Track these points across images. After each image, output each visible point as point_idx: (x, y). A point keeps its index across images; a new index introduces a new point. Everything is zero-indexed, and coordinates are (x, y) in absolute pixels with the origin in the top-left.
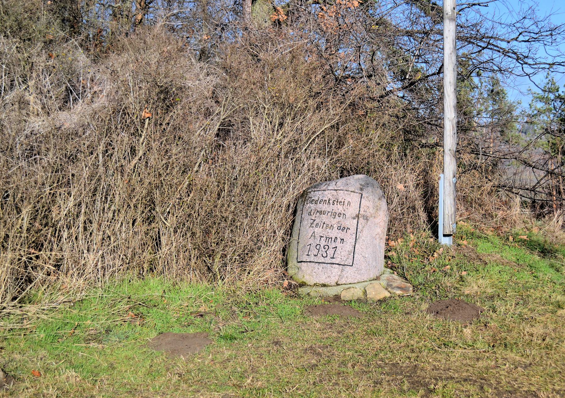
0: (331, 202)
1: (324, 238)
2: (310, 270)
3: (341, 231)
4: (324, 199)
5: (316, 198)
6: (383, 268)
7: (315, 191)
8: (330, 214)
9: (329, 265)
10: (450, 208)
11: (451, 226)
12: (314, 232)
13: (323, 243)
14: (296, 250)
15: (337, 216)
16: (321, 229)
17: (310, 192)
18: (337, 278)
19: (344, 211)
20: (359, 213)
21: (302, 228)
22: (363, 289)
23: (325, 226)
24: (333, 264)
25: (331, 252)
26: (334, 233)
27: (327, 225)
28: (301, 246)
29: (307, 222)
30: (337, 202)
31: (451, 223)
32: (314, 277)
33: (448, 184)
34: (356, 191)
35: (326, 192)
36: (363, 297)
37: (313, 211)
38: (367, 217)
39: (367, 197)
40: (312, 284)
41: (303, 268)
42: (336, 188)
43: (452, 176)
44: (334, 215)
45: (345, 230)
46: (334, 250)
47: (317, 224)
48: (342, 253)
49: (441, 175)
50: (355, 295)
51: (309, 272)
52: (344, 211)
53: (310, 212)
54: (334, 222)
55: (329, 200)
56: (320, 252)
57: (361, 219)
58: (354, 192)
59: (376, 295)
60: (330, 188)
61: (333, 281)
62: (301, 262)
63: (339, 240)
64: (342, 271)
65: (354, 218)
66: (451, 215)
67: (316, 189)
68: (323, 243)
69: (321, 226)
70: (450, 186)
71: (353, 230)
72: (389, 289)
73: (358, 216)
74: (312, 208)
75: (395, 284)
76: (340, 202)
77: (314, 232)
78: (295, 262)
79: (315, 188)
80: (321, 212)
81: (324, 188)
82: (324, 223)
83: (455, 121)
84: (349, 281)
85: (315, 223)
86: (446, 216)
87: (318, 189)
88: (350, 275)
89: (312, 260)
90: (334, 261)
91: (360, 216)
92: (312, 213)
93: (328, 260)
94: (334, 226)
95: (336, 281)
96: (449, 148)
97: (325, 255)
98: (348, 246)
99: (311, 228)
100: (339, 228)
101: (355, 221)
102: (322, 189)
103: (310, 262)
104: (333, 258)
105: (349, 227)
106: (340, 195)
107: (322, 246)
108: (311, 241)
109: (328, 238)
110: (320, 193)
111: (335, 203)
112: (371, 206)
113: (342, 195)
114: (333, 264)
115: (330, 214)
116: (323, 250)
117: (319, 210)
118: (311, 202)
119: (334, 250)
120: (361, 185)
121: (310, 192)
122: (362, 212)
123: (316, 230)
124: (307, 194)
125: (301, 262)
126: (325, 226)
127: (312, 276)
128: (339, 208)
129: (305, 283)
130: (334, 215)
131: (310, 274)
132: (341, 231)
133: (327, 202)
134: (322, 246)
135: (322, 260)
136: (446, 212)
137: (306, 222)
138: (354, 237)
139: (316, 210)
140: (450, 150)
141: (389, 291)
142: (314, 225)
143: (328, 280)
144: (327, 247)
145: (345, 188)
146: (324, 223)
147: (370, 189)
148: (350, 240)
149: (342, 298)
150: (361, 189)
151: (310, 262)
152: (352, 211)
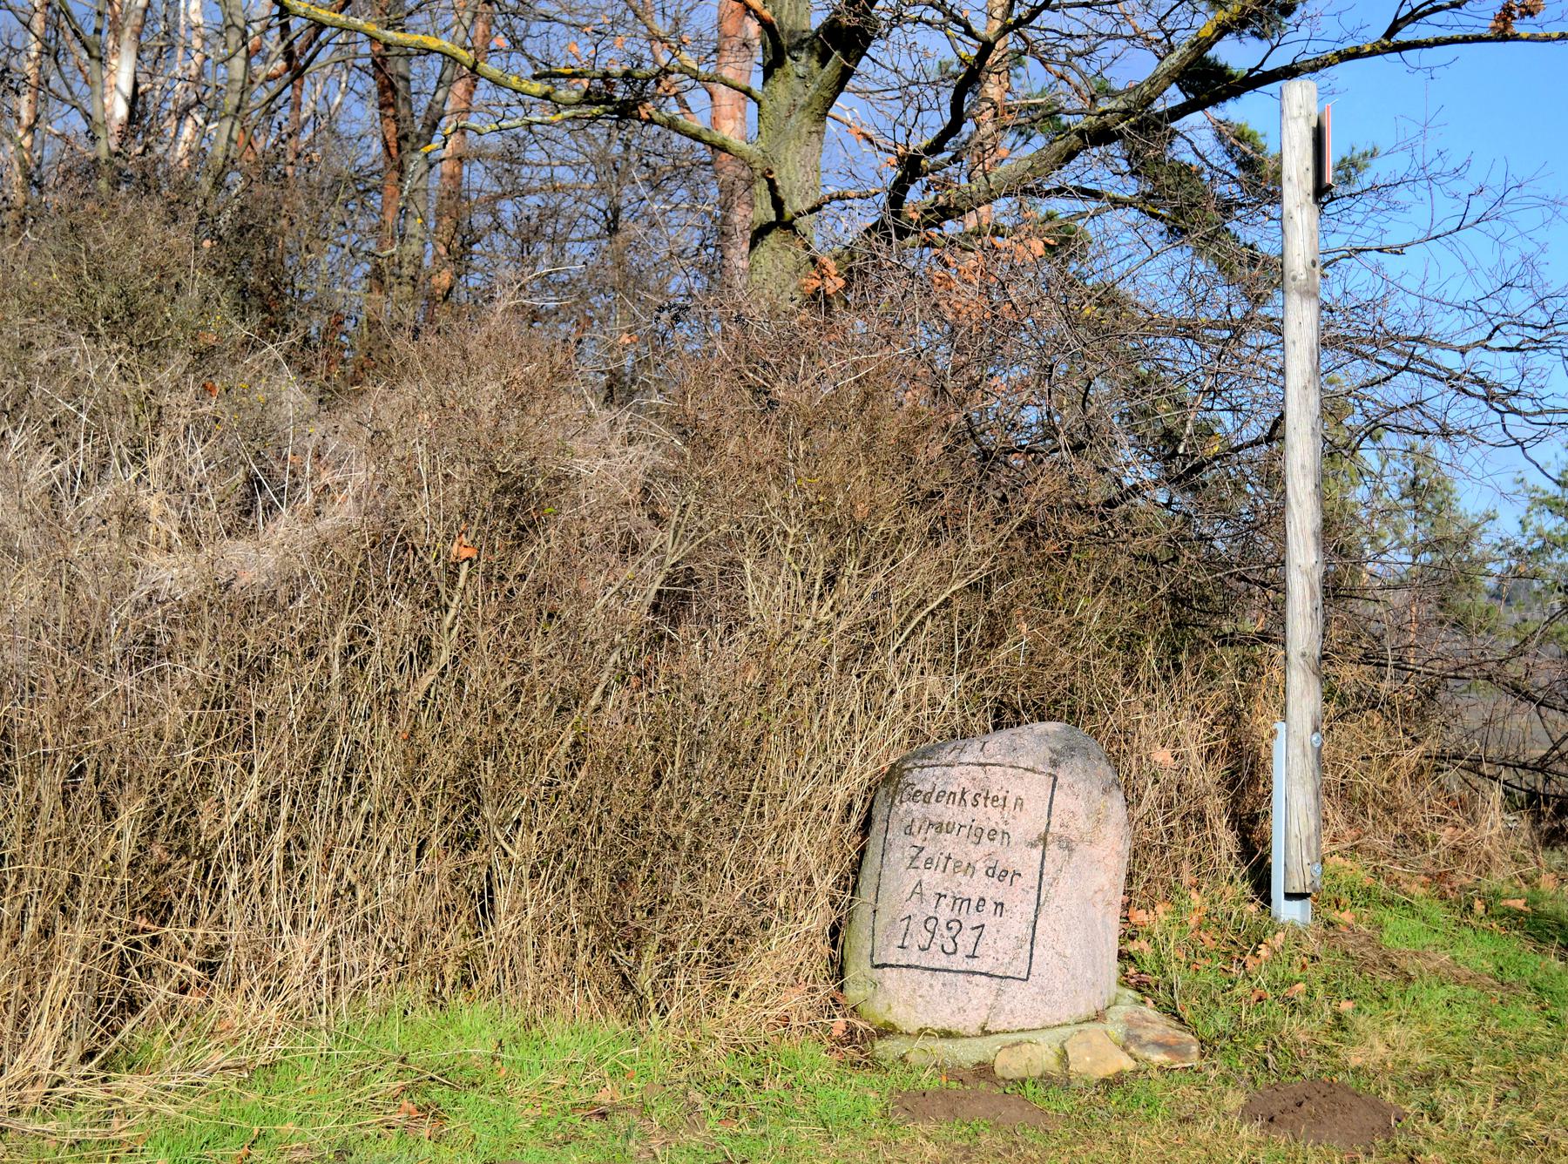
0: (969, 797)
1: (949, 900)
2: (908, 989)
3: (995, 879)
4: (949, 789)
5: (927, 787)
6: (1115, 988)
7: (923, 767)
8: (964, 831)
10: (1303, 819)
11: (1307, 869)
12: (920, 883)
13: (945, 913)
14: (868, 932)
15: (985, 839)
16: (939, 875)
17: (910, 770)
18: (984, 1013)
19: (1006, 823)
20: (1047, 831)
21: (886, 872)
22: (1056, 1046)
23: (951, 864)
24: (974, 973)
25: (966, 939)
26: (977, 886)
27: (958, 864)
28: (882, 920)
29: (899, 854)
30: (986, 798)
31: (1306, 861)
32: (920, 1009)
33: (1298, 751)
34: (1040, 768)
35: (955, 771)
36: (1057, 1069)
37: (917, 824)
38: (1070, 841)
39: (1071, 786)
40: (914, 1029)
41: (888, 984)
42: (982, 760)
43: (1309, 727)
44: (978, 834)
45: (1008, 879)
47: (929, 861)
49: (1280, 727)
50: (1035, 1062)
51: (904, 994)
52: (1006, 823)
53: (910, 827)
54: (977, 854)
55: (963, 793)
56: (938, 940)
57: (1053, 849)
58: (1033, 771)
59: (1094, 1063)
61: (972, 1023)
62: (884, 966)
63: (990, 906)
64: (998, 995)
65: (1033, 845)
66: (1308, 838)
67: (926, 762)
68: (945, 913)
70: (1305, 755)
71: (1030, 878)
72: (1133, 1049)
73: (1045, 840)
74: (916, 814)
75: (1148, 1035)
77: (920, 883)
78: (866, 966)
79: (924, 757)
80: (939, 827)
81: (950, 758)
82: (949, 858)
83: (1317, 575)
84: (1019, 1023)
86: (1293, 841)
87: (933, 762)
88: (1020, 1007)
89: (913, 962)
90: (974, 965)
91: (1049, 839)
92: (915, 829)
93: (959, 962)
94: (978, 866)
95: (980, 1022)
96: (1300, 649)
97: (950, 948)
98: (1016, 923)
100: (991, 872)
101: (1036, 854)
102: (944, 761)
103: (908, 966)
105: (1018, 868)
106: (993, 779)
107: (942, 922)
108: (911, 908)
109: (960, 901)
110: (938, 771)
111: (981, 800)
112: (1081, 812)
113: (998, 780)
114: (974, 973)
116: (946, 933)
117: (934, 819)
118: (913, 798)
120: (1053, 751)
121: (910, 770)
122: (1055, 828)
123: (926, 876)
124: (901, 776)
125: (884, 966)
126: (951, 864)
127: (915, 1007)
128: (990, 816)
129: (893, 1025)
130: (978, 834)
131: (904, 999)
132: (995, 879)
134: (942, 922)
135: (942, 961)
136: (1294, 830)
139: (925, 819)
140: (1303, 655)
141: (1131, 1055)
142: (920, 863)
143: (959, 1018)
145: (1008, 760)
146: (949, 858)
147: (1078, 762)
148: (1021, 908)
149: (999, 1073)
150: (1054, 764)
151: (908, 966)
152: (1028, 823)
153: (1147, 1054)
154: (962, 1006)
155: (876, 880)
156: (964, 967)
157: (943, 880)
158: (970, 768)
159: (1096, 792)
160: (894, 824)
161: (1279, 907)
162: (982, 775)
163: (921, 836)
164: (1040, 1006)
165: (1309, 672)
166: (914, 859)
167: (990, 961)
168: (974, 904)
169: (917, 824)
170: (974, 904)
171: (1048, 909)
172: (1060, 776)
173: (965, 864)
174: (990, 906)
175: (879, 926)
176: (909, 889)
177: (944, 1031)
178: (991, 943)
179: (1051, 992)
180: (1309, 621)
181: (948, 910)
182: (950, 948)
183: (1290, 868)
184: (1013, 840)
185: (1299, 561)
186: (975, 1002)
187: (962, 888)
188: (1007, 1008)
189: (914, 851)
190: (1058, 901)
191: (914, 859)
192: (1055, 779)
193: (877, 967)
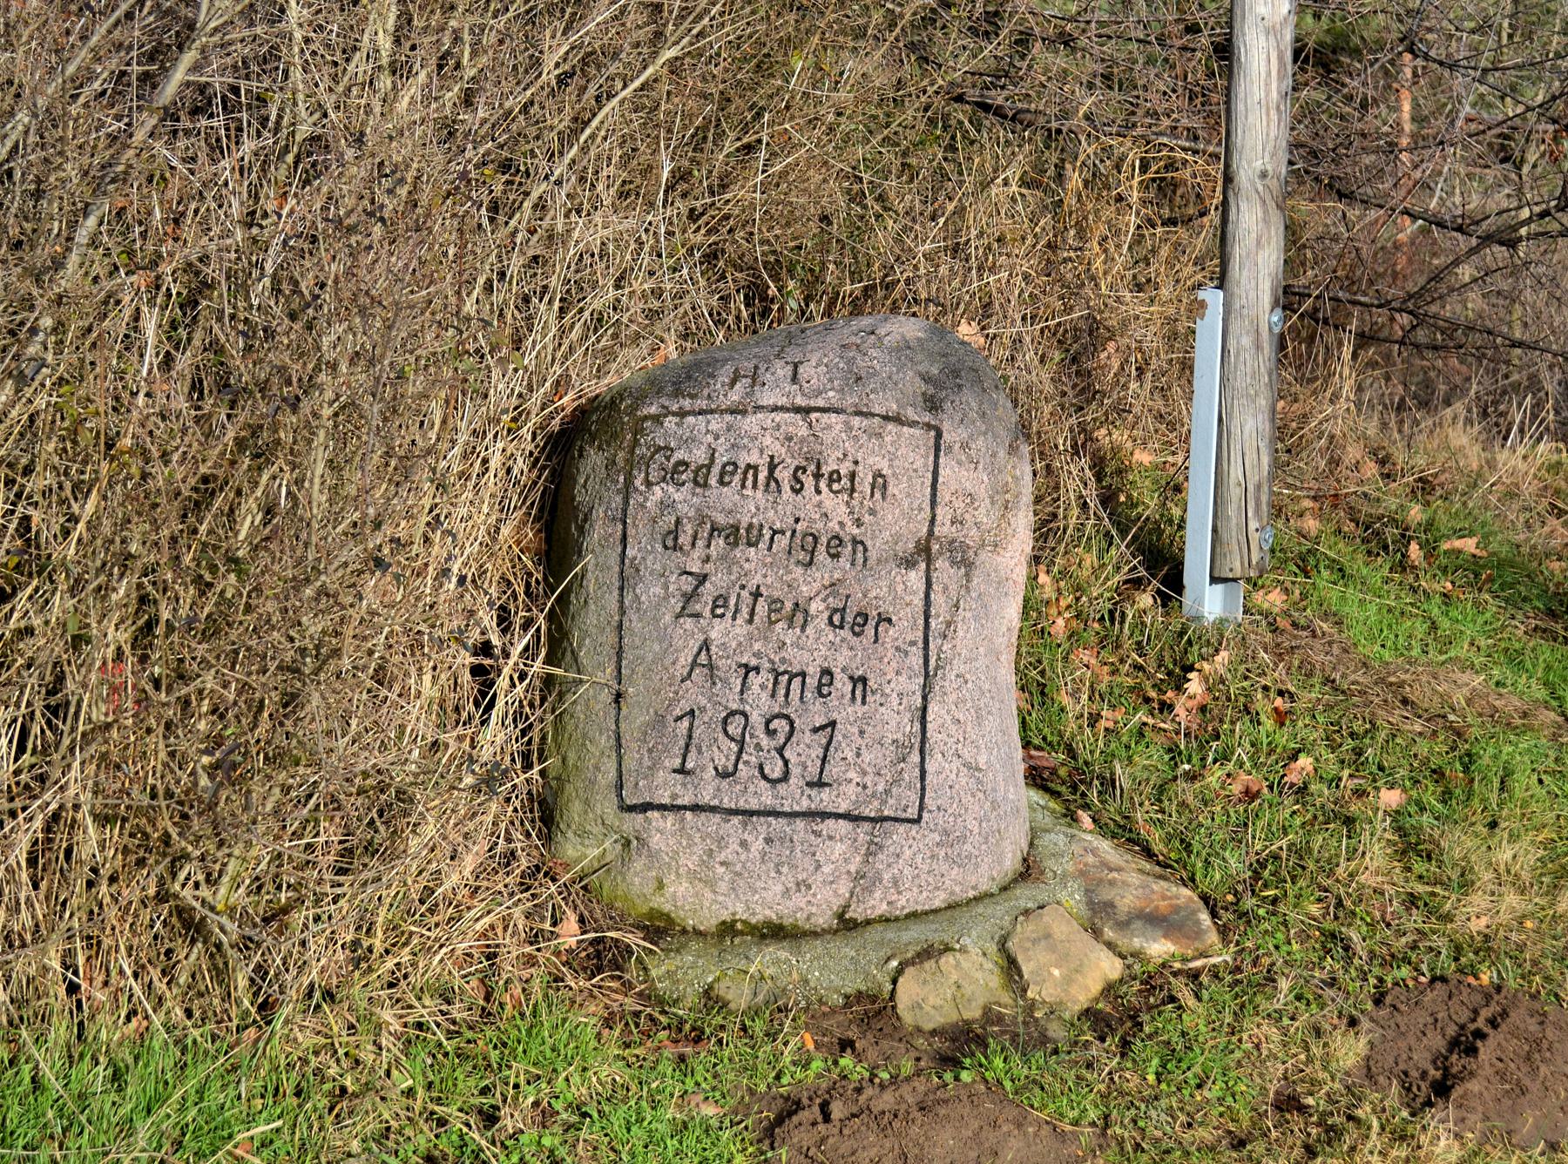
0: (784, 475)
1: (765, 677)
2: (699, 850)
3: (845, 633)
4: (744, 459)
5: (699, 455)
7: (682, 414)
8: (782, 542)
9: (800, 824)
10: (1251, 457)
11: (1254, 537)
12: (706, 645)
13: (760, 703)
14: (605, 741)
15: (821, 555)
16: (741, 629)
17: (657, 419)
18: (844, 888)
19: (858, 523)
20: (931, 533)
21: (634, 622)
22: (992, 948)
23: (762, 607)
24: (825, 815)
25: (804, 752)
26: (815, 647)
27: (775, 605)
28: (636, 718)
29: (656, 589)
30: (817, 476)
31: (1253, 525)
32: (723, 887)
33: (1246, 341)
34: (911, 413)
35: (751, 423)
36: (1006, 998)
37: (689, 529)
38: (965, 548)
39: (965, 446)
40: (709, 922)
41: (656, 841)
42: (800, 401)
43: (1267, 300)
44: (808, 547)
45: (869, 630)
46: (822, 738)
47: (720, 601)
48: (867, 757)
49: (1213, 298)
50: (968, 990)
51: (690, 862)
52: (858, 523)
53: (675, 532)
54: (810, 584)
55: (772, 467)
57: (941, 563)
58: (897, 420)
59: (1068, 980)
60: (768, 398)
61: (819, 907)
62: (646, 807)
63: (842, 685)
64: (869, 854)
65: (909, 564)
66: (1258, 487)
67: (687, 403)
68: (760, 703)
69: (745, 611)
70: (1258, 347)
71: (905, 628)
72: (1109, 933)
73: (928, 550)
74: (683, 509)
75: (1127, 901)
76: (834, 477)
77: (706, 645)
78: (607, 807)
79: (677, 393)
80: (733, 535)
81: (735, 396)
84: (907, 901)
86: (1235, 493)
87: (702, 403)
88: (914, 875)
89: (706, 798)
90: (824, 799)
91: (935, 547)
92: (685, 539)
93: (795, 796)
94: (814, 607)
95: (836, 904)
96: (1258, 164)
97: (775, 770)
99: (688, 623)
101: (915, 578)
102: (725, 403)
103: (696, 808)
104: (820, 784)
106: (827, 438)
107: (756, 718)
108: (694, 694)
110: (716, 423)
111: (809, 481)
112: (982, 492)
113: (837, 439)
114: (825, 815)
115: (782, 542)
116: (765, 741)
117: (721, 519)
118: (673, 474)
119: (822, 738)
120: (926, 379)
121: (657, 419)
122: (944, 529)
123: (717, 631)
124: (638, 431)
125: (646, 807)
126: (762, 607)
127: (711, 884)
128: (830, 510)
129: (667, 917)
130: (808, 547)
131: (690, 873)
132: (845, 633)
133: (762, 476)
136: (1236, 473)
137: (657, 590)
138: (916, 660)
139: (701, 519)
140: (1264, 175)
141: (1110, 945)
142: (703, 606)
143: (799, 900)
144: (780, 725)
145: (850, 401)
146: (757, 595)
147: (969, 398)
148: (899, 684)
149: (908, 1018)
150: (933, 405)
151: (696, 808)
152: (896, 522)
153: (1137, 942)
154: (810, 878)
155: (612, 638)
156: (805, 804)
157: (750, 638)
158: (779, 417)
159: (1002, 454)
160: (639, 532)
161: (1199, 601)
162: (803, 431)
163: (698, 553)
164: (944, 868)
165: (1271, 205)
166: (689, 598)
167: (851, 790)
168: (811, 682)
169: (689, 529)
170: (811, 682)
171: (947, 682)
172: (946, 427)
173: (789, 605)
174: (842, 685)
175: (629, 731)
176: (685, 659)
177: (768, 924)
178: (850, 755)
179: (962, 839)
180: (1274, 116)
181: (765, 696)
182: (775, 770)
183: (1224, 535)
184: (873, 554)
185: (1262, 10)
186: (826, 869)
187: (789, 653)
188: (886, 876)
189: (687, 584)
190: (958, 666)
191: (689, 598)
192: (939, 435)
193: (631, 809)
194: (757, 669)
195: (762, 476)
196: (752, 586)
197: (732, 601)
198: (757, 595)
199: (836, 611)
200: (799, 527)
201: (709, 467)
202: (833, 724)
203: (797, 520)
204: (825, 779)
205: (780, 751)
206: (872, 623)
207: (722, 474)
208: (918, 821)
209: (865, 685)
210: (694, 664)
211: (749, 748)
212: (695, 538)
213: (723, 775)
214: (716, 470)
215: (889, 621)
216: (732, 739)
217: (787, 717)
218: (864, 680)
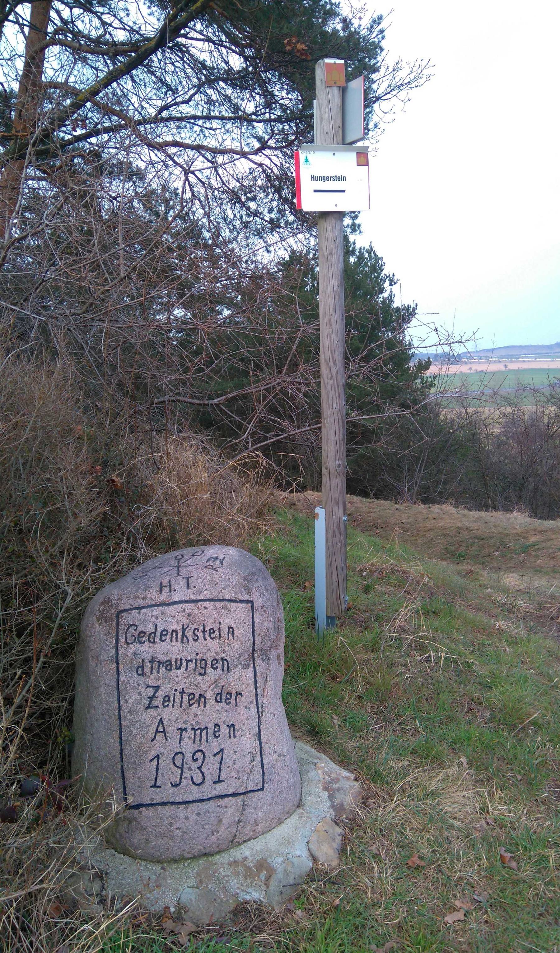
0: (189, 633)
1: (191, 733)
5: (150, 628)
6: (293, 742)
9: (212, 803)
12: (161, 720)
15: (209, 670)
23: (186, 698)
25: (210, 767)
30: (204, 632)
42: (193, 597)
45: (233, 701)
47: (166, 699)
48: (239, 764)
55: (184, 630)
56: (187, 774)
60: (176, 597)
62: (138, 806)
63: (224, 730)
68: (188, 747)
69: (178, 701)
76: (212, 631)
77: (161, 720)
80: (168, 665)
82: (182, 692)
83: (342, 381)
85: (160, 694)
90: (220, 789)
92: (147, 670)
93: (208, 790)
97: (198, 779)
98: (247, 741)
99: (152, 712)
104: (219, 781)
105: (238, 688)
107: (188, 756)
109: (199, 730)
115: (192, 665)
117: (163, 658)
119: (218, 757)
125: (138, 806)
128: (211, 648)
130: (201, 665)
133: (180, 635)
134: (188, 756)
135: (195, 793)
137: (136, 697)
138: (254, 710)
142: (158, 702)
156: (214, 793)
158: (184, 606)
166: (152, 698)
168: (211, 731)
170: (211, 731)
173: (197, 695)
174: (224, 730)
181: (190, 742)
182: (198, 779)
189: (150, 692)
194: (185, 729)
195: (180, 635)
196: (180, 689)
197: (172, 699)
198: (182, 692)
199: (218, 694)
200: (198, 657)
201: (155, 633)
202: (222, 750)
203: (197, 654)
204: (221, 779)
205: (200, 768)
206: (233, 697)
207: (162, 635)
208: (262, 789)
209: (234, 728)
210: (157, 731)
211: (186, 770)
212: (152, 668)
213: (175, 785)
214: (158, 634)
215: (241, 694)
216: (178, 767)
217: (201, 751)
218: (233, 725)
